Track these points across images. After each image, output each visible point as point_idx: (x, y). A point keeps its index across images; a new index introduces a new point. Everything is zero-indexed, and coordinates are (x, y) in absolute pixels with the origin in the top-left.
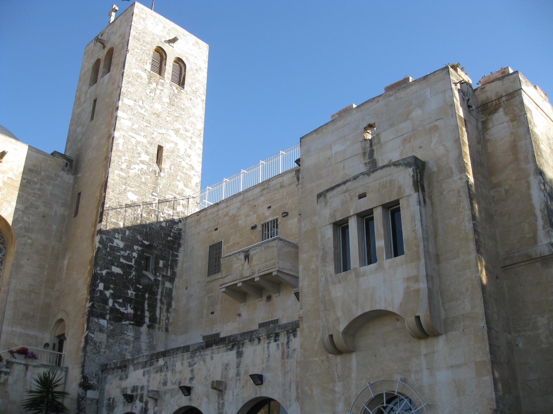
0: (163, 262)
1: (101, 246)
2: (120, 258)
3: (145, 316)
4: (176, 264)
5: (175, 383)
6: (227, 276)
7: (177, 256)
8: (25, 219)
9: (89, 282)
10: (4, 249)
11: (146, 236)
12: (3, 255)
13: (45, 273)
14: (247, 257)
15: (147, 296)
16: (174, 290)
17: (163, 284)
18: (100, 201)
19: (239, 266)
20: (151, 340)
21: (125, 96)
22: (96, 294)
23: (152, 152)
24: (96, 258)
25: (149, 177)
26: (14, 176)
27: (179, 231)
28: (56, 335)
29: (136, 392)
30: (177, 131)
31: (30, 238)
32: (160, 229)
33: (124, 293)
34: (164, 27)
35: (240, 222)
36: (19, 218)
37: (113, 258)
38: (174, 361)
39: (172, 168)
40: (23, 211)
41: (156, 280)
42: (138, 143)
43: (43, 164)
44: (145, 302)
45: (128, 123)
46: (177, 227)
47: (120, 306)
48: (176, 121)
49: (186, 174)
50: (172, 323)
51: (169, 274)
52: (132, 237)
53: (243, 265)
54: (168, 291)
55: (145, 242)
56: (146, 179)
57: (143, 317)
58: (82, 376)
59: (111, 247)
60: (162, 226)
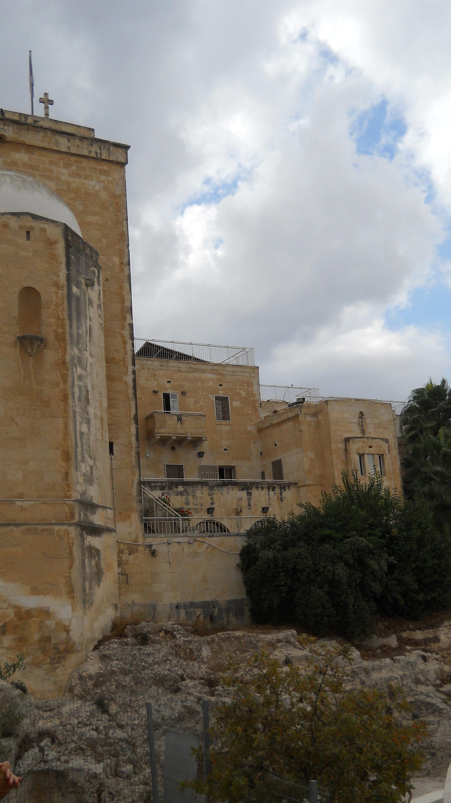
5: (197, 505)
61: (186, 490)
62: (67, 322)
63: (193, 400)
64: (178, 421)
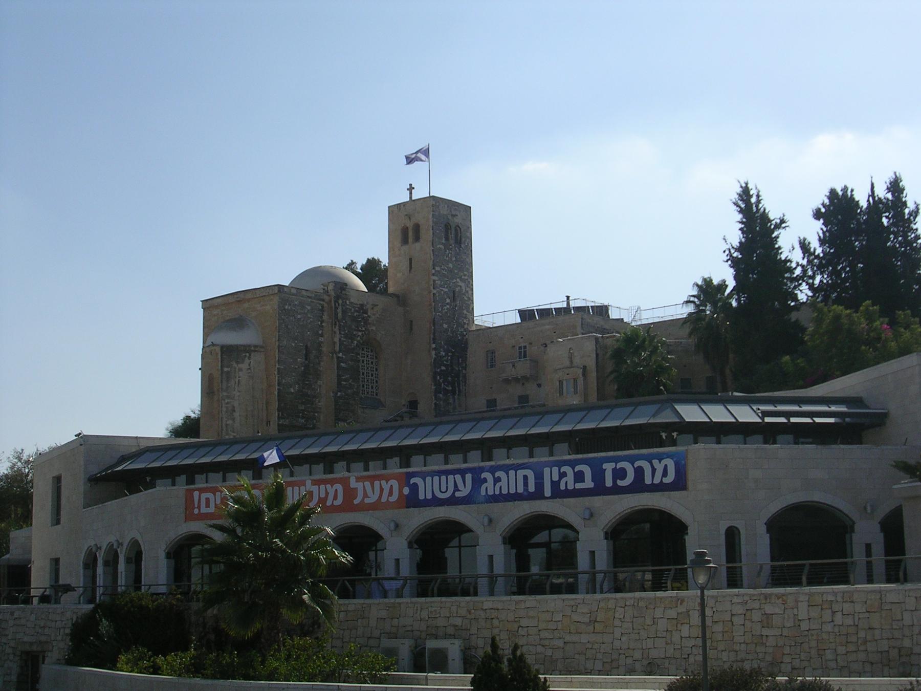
14: (513, 366)
17: (462, 371)
30: (460, 278)
34: (448, 207)
40: (385, 335)
51: (464, 365)
59: (441, 357)
62: (220, 384)
63: (536, 348)
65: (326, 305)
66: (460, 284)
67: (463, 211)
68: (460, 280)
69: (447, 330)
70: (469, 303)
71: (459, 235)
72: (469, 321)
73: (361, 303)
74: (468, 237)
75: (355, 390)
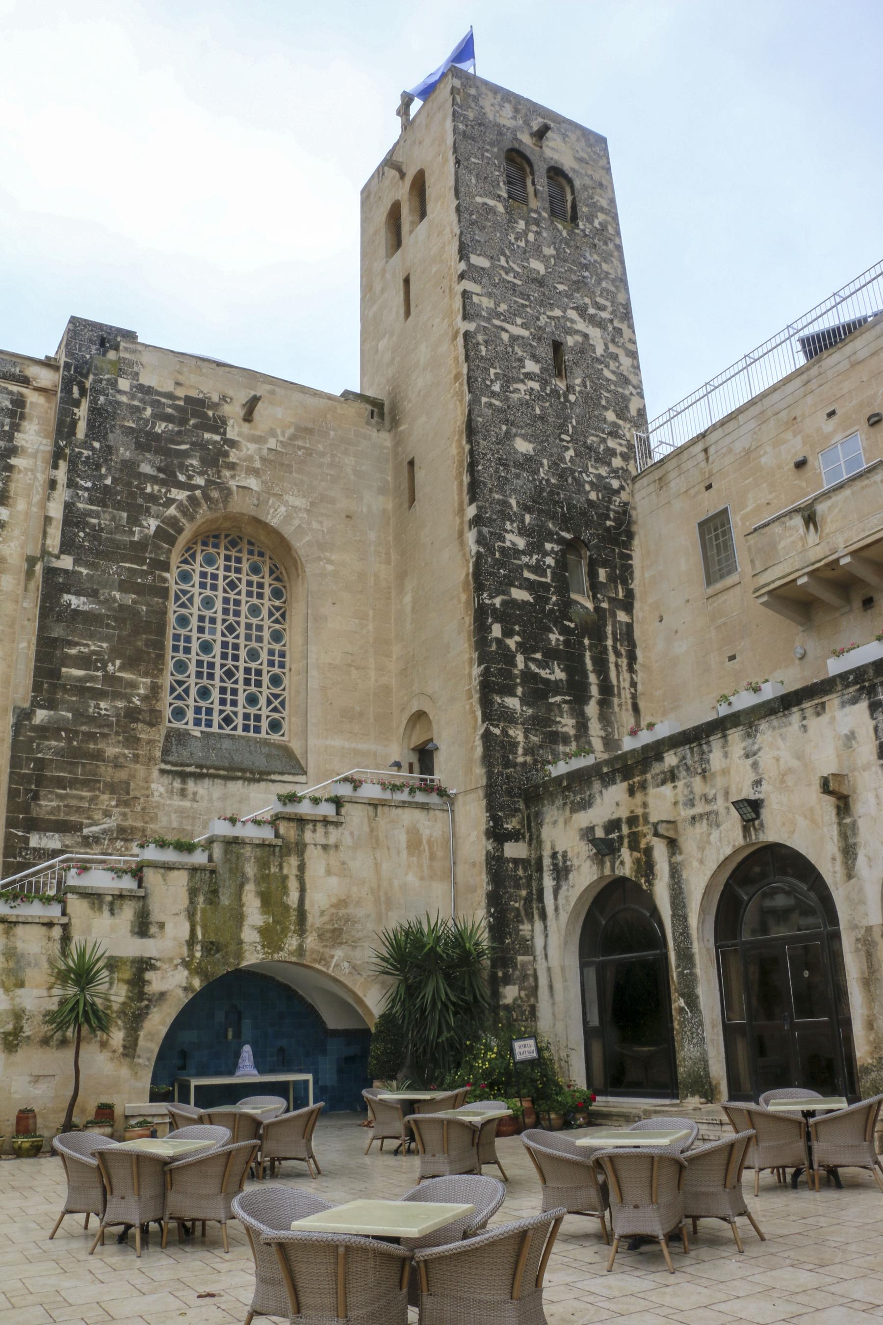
0: (606, 572)
1: (482, 550)
2: (522, 571)
3: (590, 684)
4: (632, 572)
6: (766, 569)
7: (630, 557)
8: (315, 525)
9: (470, 626)
10: (283, 590)
11: (565, 522)
12: (284, 602)
13: (371, 627)
14: (810, 519)
15: (586, 642)
16: (635, 625)
17: (614, 616)
18: (461, 463)
19: (793, 542)
20: (610, 730)
21: (470, 249)
22: (490, 646)
23: (544, 355)
24: (477, 573)
25: (547, 404)
26: (279, 444)
27: (624, 506)
28: (412, 747)
29: (619, 832)
30: (582, 311)
31: (330, 562)
32: (588, 505)
33: (543, 640)
34: (516, 111)
35: (763, 460)
36: (303, 525)
37: (510, 571)
38: (703, 753)
39: (588, 383)
40: (308, 511)
41: (597, 609)
42: (514, 339)
43: (328, 416)
44: (585, 655)
45: (486, 303)
46: (618, 500)
47: (539, 667)
48: (578, 290)
49: (615, 393)
50: (643, 694)
51: (621, 595)
52: (537, 526)
53: (804, 539)
54: (624, 629)
55: (563, 534)
56: (542, 409)
57: (585, 686)
58: (488, 814)
59: (503, 550)
60: (590, 500)
61: (684, 758)
64: (808, 528)
65: (32, 397)
66: (581, 325)
67: (578, 140)
68: (581, 316)
69: (529, 463)
70: (627, 392)
71: (569, 198)
72: (631, 447)
73: (193, 394)
74: (602, 209)
75: (136, 700)
